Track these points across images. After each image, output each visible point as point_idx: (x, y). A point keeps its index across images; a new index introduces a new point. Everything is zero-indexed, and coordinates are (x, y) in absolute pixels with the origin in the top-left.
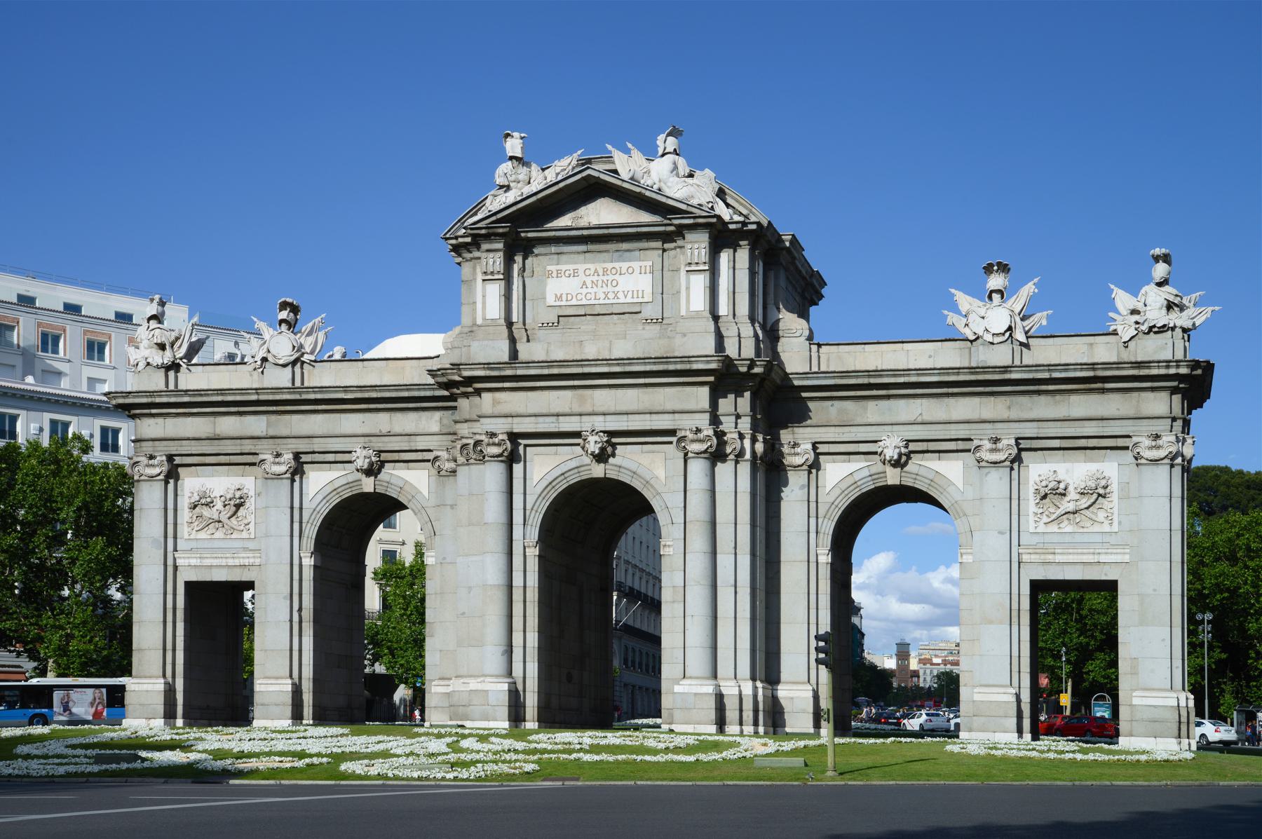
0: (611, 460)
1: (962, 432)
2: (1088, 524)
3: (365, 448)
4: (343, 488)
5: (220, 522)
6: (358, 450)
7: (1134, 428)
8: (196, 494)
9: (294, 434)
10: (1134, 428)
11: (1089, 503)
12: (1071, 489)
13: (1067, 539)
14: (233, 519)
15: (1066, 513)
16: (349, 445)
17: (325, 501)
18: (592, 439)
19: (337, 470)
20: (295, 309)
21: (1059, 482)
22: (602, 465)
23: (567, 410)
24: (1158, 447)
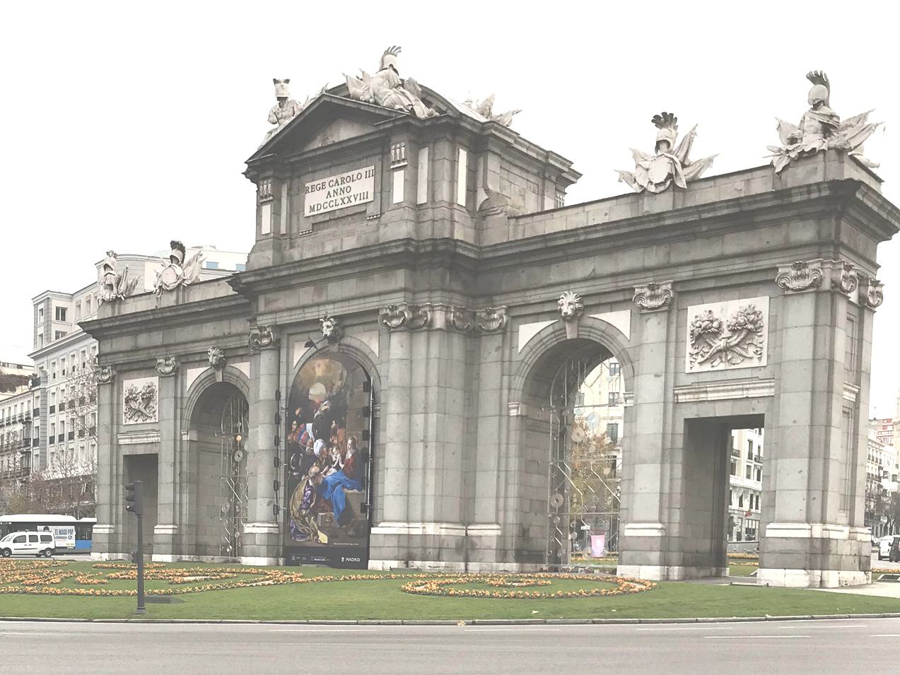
0: (347, 341)
6: (211, 350)
9: (177, 341)
11: (739, 340)
12: (724, 326)
13: (720, 377)
15: (720, 351)
18: (325, 324)
19: (203, 367)
21: (712, 322)
23: (310, 302)
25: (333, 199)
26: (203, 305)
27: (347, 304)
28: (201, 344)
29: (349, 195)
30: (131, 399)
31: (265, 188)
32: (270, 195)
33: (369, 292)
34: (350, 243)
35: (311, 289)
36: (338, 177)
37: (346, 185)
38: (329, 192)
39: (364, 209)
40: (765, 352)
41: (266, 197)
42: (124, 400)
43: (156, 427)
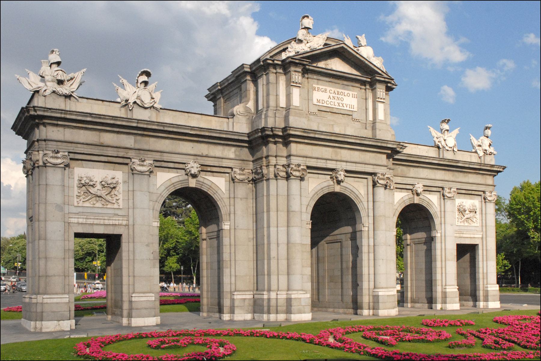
1: (440, 184)
2: (471, 223)
4: (177, 183)
5: (101, 197)
6: (191, 163)
7: (485, 189)
8: (85, 179)
9: (151, 148)
10: (485, 189)
14: (108, 196)
16: (185, 160)
17: (166, 190)
20: (148, 74)
23: (330, 158)
24: (491, 196)
25: (332, 100)
26: (195, 130)
27: (354, 164)
28: (178, 156)
29: (343, 102)
30: (90, 185)
31: (297, 78)
32: (299, 83)
33: (367, 162)
34: (349, 131)
36: (336, 90)
37: (340, 96)
38: (330, 97)
39: (351, 114)
40: (478, 221)
43: (120, 212)
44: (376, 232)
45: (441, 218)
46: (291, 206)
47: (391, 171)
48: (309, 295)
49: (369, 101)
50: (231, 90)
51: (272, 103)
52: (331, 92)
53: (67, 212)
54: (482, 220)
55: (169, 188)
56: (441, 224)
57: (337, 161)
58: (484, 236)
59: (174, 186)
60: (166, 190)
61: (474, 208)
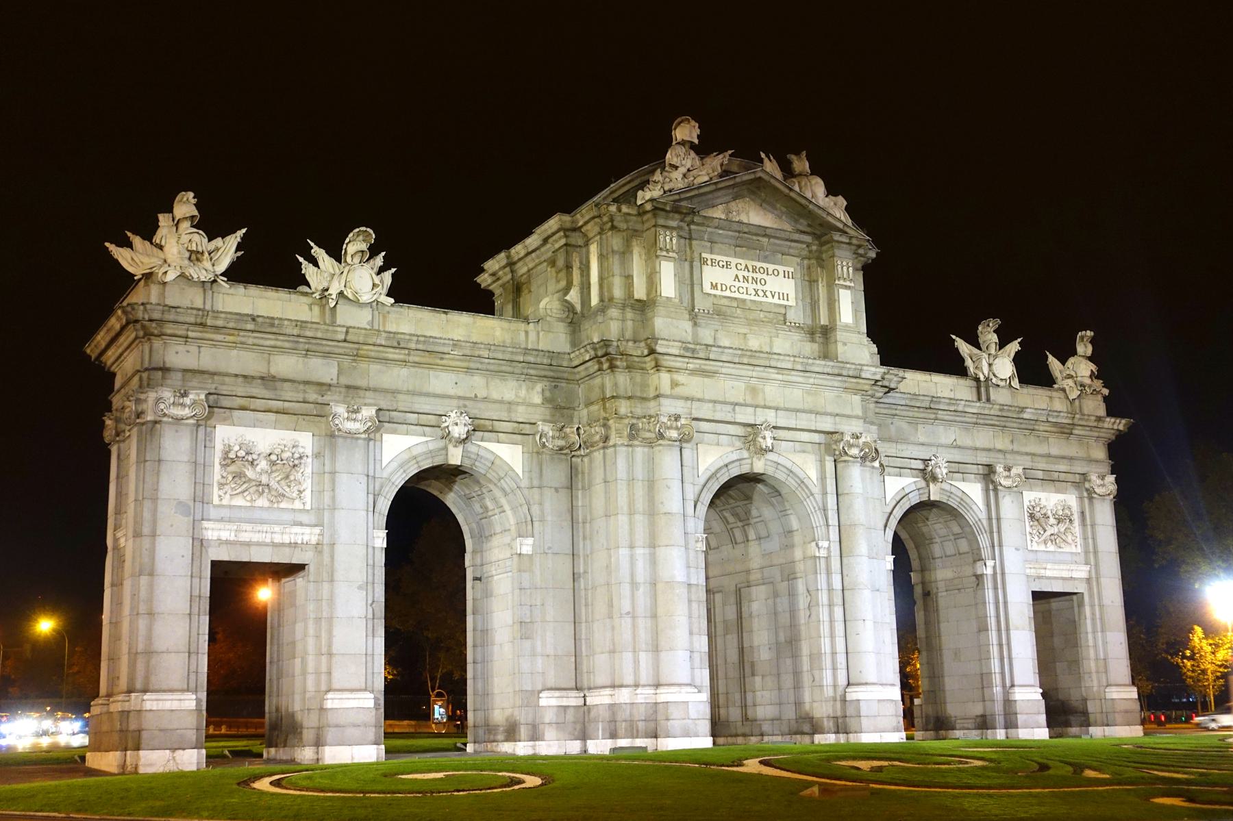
0: (770, 456)
2: (1062, 545)
3: (462, 413)
6: (453, 415)
8: (237, 448)
22: (762, 461)
23: (741, 401)
24: (1103, 485)
25: (741, 284)
29: (765, 288)
30: (247, 461)
31: (668, 241)
35: (741, 385)
36: (750, 264)
37: (759, 276)
38: (737, 276)
41: (667, 251)
42: (217, 461)
43: (305, 518)
44: (845, 560)
45: (991, 532)
46: (662, 503)
47: (874, 428)
48: (705, 696)
49: (820, 285)
50: (531, 266)
51: (618, 293)
52: (739, 265)
53: (198, 517)
54: (1085, 539)
55: (406, 467)
56: (993, 546)
57: (756, 406)
58: (1094, 575)
59: (417, 463)
60: (402, 470)
61: (1067, 511)
